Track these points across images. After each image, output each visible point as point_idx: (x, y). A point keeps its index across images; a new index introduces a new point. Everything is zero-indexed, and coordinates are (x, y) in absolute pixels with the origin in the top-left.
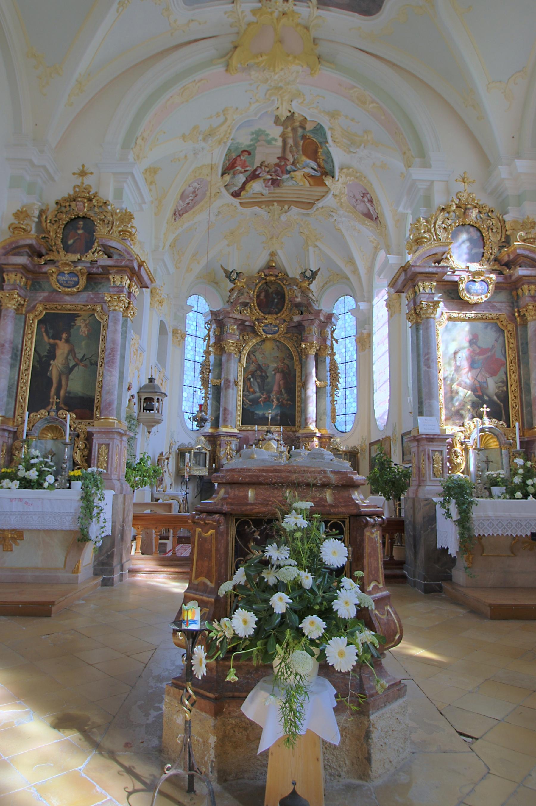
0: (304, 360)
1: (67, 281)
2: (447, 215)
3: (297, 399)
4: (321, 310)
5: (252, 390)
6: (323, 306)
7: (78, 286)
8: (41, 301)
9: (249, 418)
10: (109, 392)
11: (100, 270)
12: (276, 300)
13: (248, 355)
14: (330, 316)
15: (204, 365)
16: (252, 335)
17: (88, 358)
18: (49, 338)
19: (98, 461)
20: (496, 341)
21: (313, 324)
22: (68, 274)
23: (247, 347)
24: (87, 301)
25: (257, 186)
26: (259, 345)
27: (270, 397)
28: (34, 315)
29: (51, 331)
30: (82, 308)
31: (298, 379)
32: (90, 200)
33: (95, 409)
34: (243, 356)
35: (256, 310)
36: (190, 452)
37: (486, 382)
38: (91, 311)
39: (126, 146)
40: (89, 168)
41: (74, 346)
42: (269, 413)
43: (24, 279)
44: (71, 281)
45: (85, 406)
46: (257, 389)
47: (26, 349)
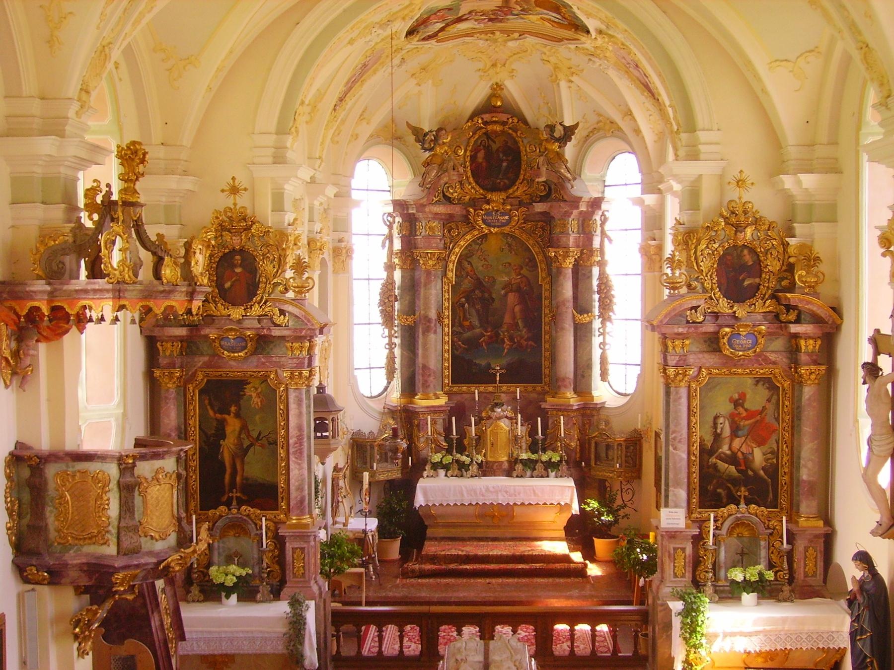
0: (554, 270)
1: (233, 347)
2: (714, 234)
3: (545, 337)
4: (581, 198)
5: (467, 323)
6: (584, 187)
8: (200, 367)
9: (463, 370)
12: (505, 164)
13: (459, 262)
14: (596, 203)
15: (388, 285)
16: (463, 230)
18: (215, 413)
19: (293, 568)
20: (769, 400)
21: (569, 217)
23: (457, 250)
24: (257, 367)
25: (462, 26)
26: (478, 244)
27: (497, 335)
31: (545, 303)
32: (248, 229)
33: (280, 499)
34: (451, 266)
35: (470, 184)
36: (372, 447)
37: (752, 453)
39: (282, 130)
40: (242, 180)
42: (498, 371)
45: (266, 495)
46: (476, 323)
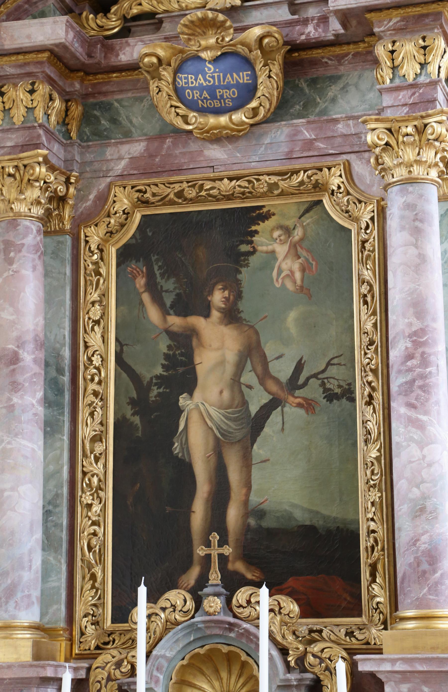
1: (212, 90)
7: (254, 104)
8: (121, 176)
10: (422, 510)
11: (335, 26)
17: (315, 376)
18: (165, 312)
22: (216, 60)
28: (102, 230)
29: (169, 285)
30: (273, 186)
38: (307, 192)
41: (257, 333)
43: (57, 103)
44: (228, 87)
47: (90, 360)
